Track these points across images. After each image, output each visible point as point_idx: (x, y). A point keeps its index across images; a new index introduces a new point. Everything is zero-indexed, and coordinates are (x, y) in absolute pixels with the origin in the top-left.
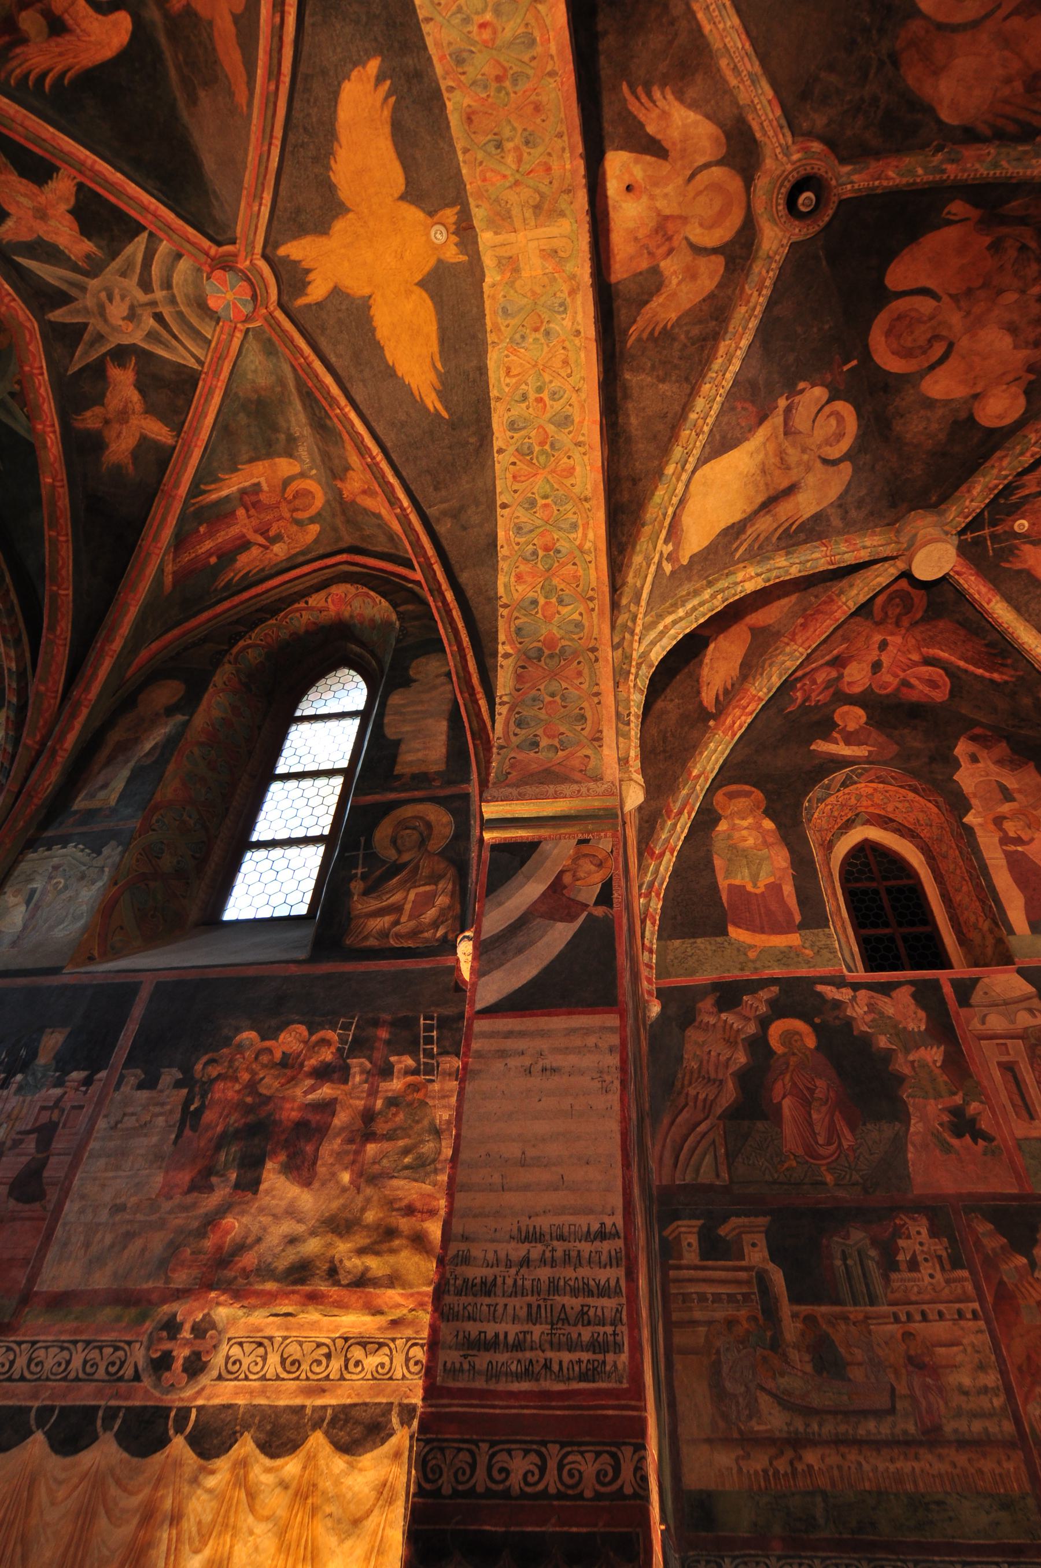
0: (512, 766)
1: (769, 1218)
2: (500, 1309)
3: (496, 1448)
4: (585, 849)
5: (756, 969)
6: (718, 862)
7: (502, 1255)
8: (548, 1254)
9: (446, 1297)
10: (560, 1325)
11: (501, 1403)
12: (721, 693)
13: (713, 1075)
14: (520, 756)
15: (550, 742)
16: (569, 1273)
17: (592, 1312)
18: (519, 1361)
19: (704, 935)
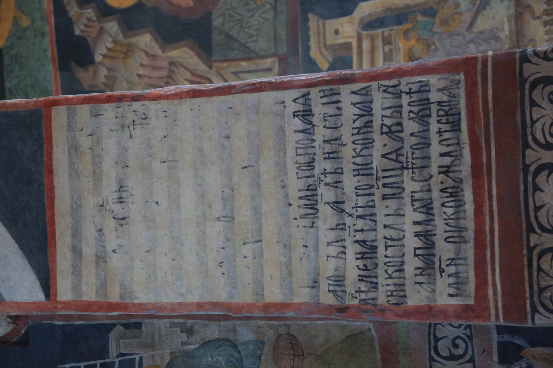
1: (310, 16)
2: (390, 233)
3: (535, 225)
5: (42, 18)
7: (332, 236)
8: (329, 179)
9: (379, 302)
10: (403, 159)
11: (488, 223)
13: (165, 73)
16: (348, 152)
17: (388, 122)
18: (443, 205)
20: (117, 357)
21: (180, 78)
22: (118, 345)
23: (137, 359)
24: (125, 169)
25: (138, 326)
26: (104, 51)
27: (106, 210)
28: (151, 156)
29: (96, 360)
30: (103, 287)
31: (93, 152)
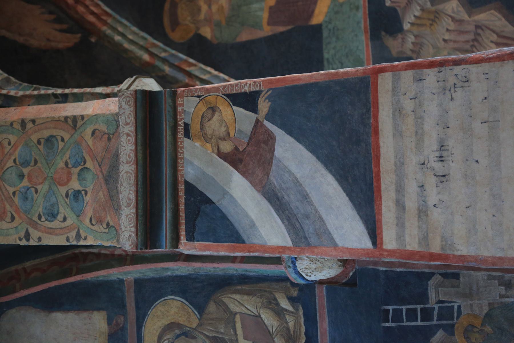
0: (100, 221)
4: (195, 128)
6: (245, 37)
12: (58, 26)
13: (471, 37)
14: (89, 212)
15: (75, 177)
19: (320, 50)
20: (436, 303)
21: (486, 40)
22: (437, 292)
23: (456, 307)
24: (446, 129)
25: (456, 276)
26: (412, 19)
27: (427, 168)
28: (471, 117)
29: (416, 304)
30: (425, 239)
31: (415, 114)
